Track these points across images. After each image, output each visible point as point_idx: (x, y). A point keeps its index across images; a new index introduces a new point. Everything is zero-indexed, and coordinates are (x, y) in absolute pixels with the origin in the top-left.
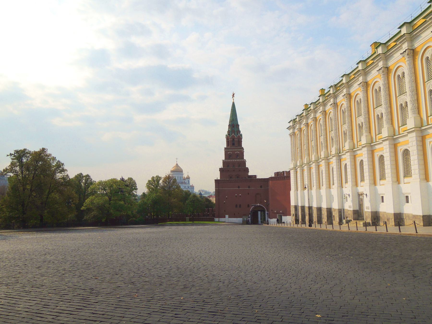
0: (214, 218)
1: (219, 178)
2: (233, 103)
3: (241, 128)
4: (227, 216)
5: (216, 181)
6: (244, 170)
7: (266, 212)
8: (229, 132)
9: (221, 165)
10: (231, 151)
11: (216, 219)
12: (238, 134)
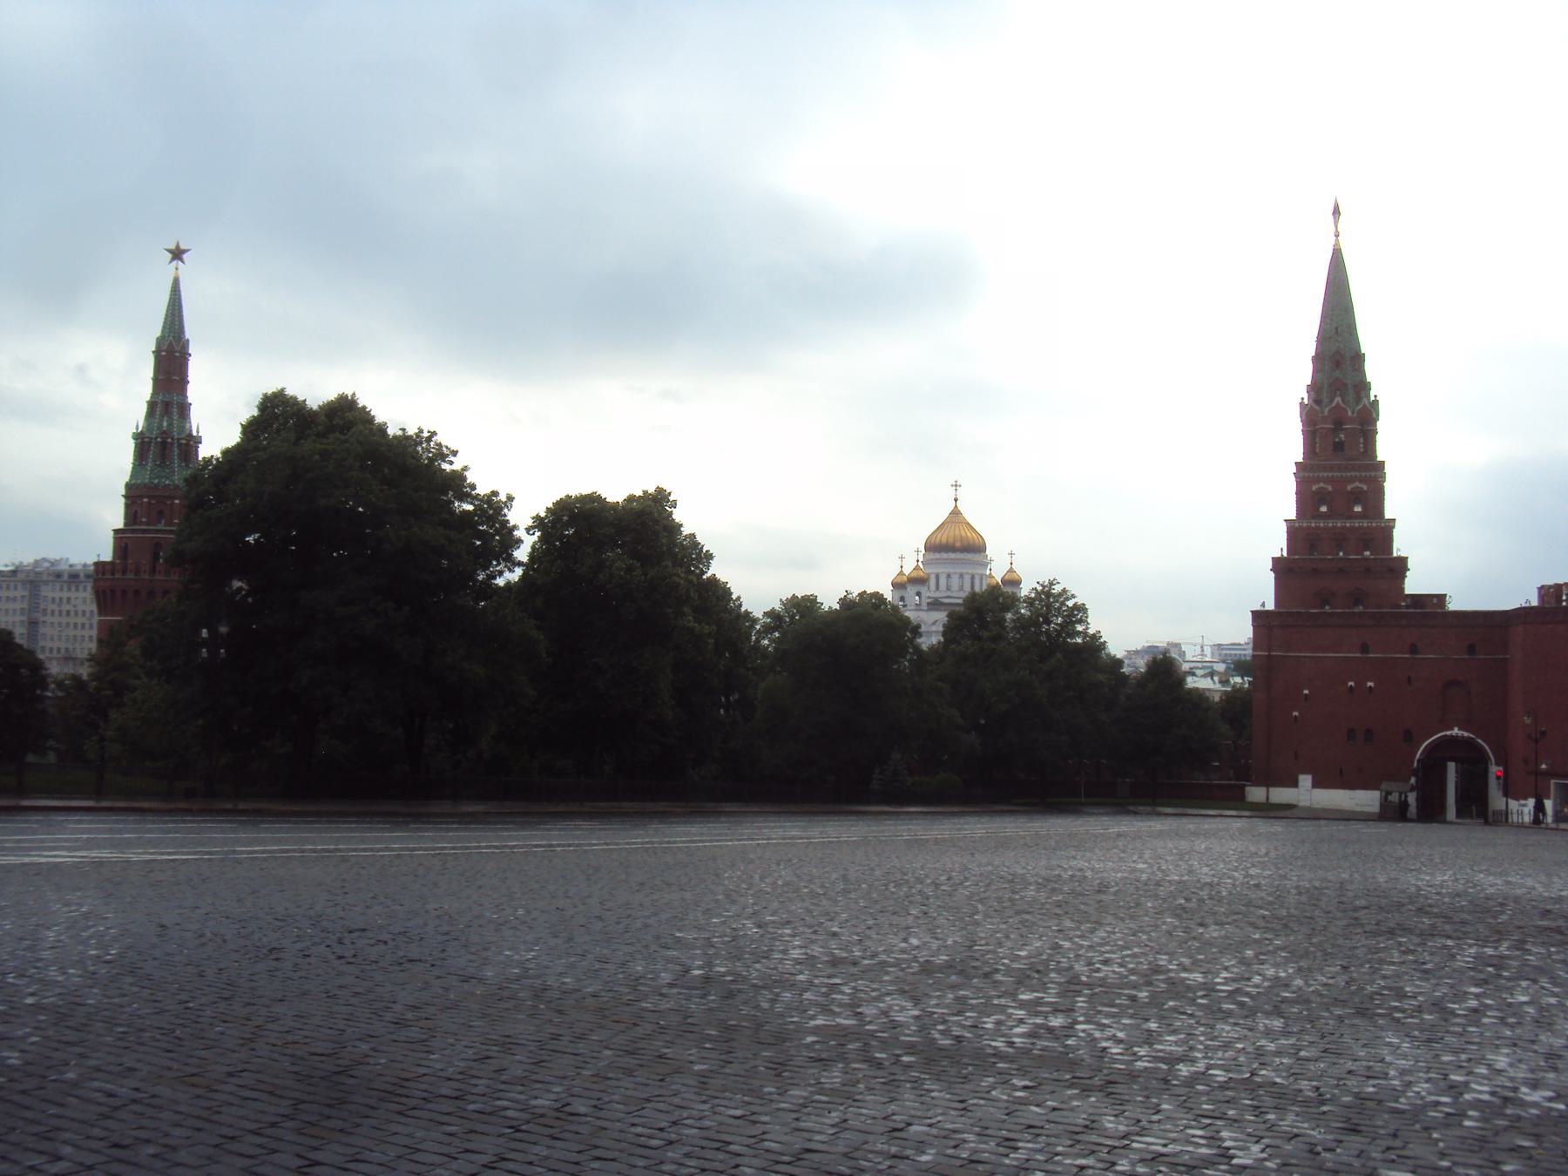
0: (1242, 788)
1: (1270, 606)
2: (1337, 244)
3: (1372, 371)
4: (1305, 780)
5: (1259, 617)
6: (1391, 570)
7: (1494, 769)
8: (1314, 388)
9: (1278, 545)
10: (1326, 480)
11: (1256, 794)
12: (1358, 399)
